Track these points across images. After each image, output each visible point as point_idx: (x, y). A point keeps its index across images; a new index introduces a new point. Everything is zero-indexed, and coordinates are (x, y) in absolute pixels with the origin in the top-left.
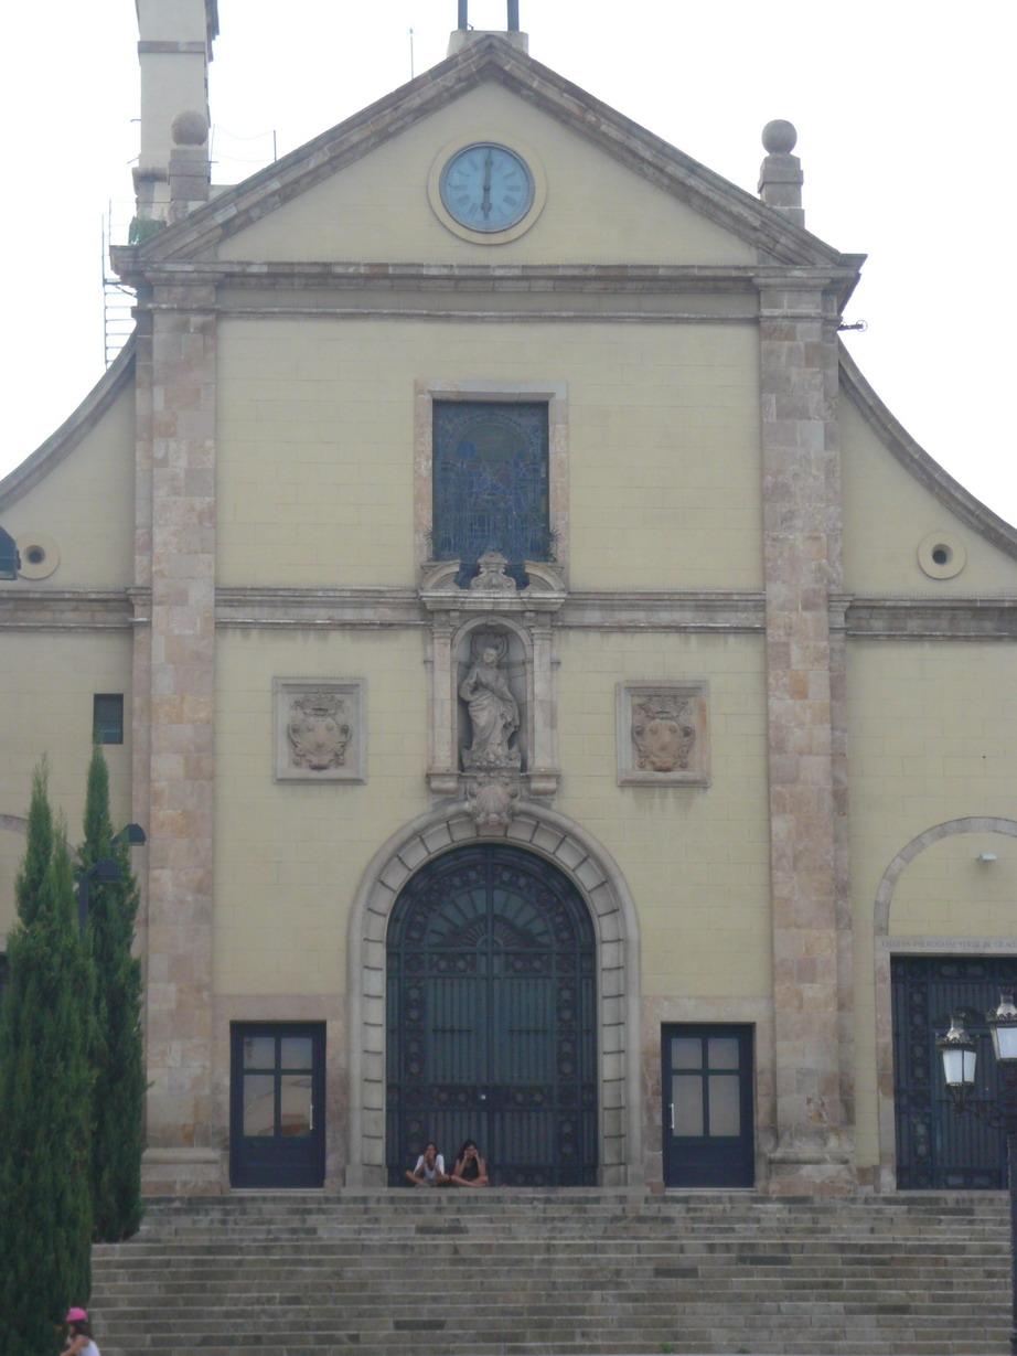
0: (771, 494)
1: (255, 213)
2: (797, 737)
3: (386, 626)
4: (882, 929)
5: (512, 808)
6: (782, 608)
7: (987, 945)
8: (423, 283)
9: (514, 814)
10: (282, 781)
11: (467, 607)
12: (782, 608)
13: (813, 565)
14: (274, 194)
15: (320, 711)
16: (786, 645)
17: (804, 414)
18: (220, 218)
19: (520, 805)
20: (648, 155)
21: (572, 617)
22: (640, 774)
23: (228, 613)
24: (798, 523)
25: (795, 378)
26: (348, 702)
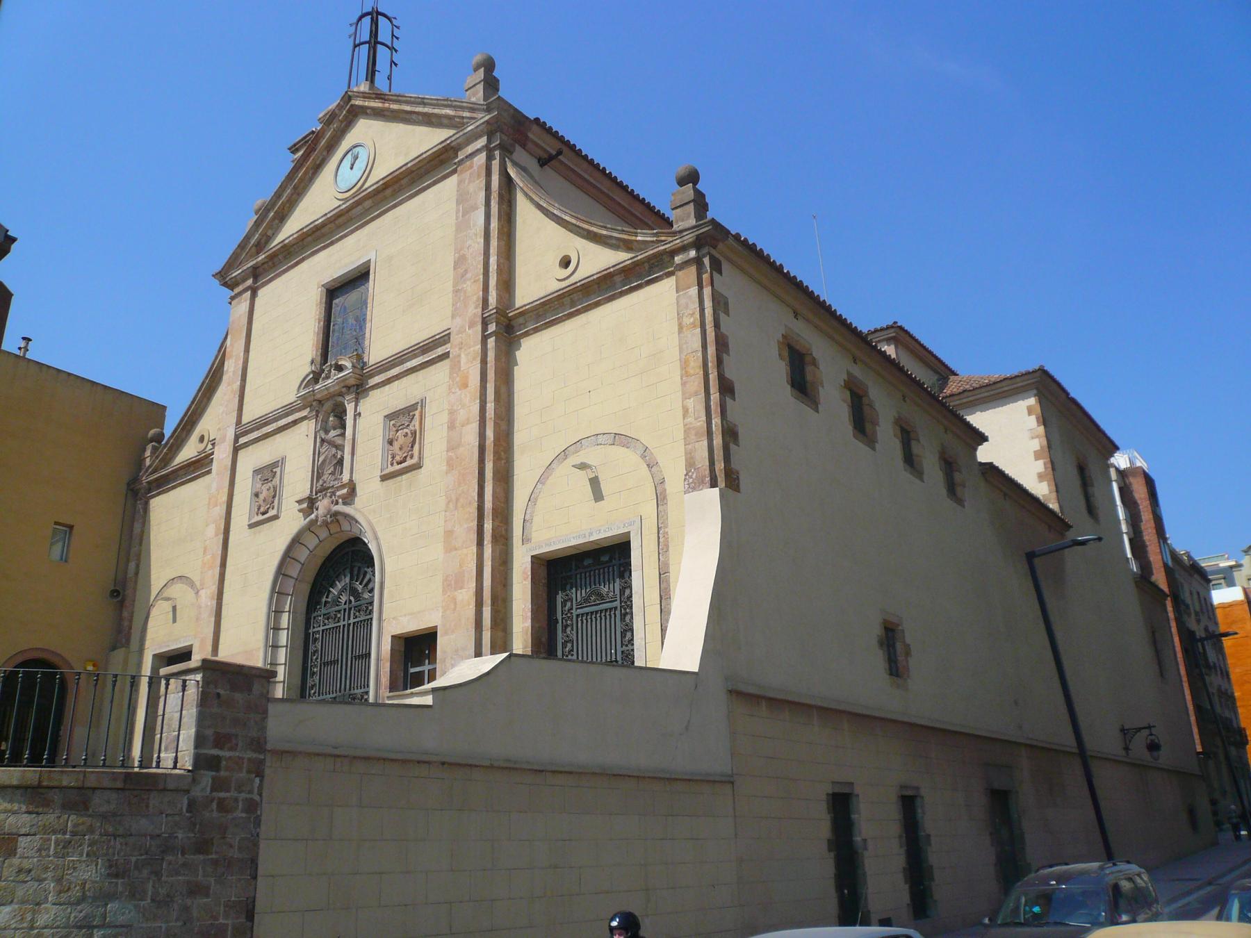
0: (460, 262)
1: (270, 233)
2: (462, 415)
3: (295, 422)
4: (525, 540)
5: (329, 511)
6: (459, 332)
7: (591, 534)
8: (323, 230)
9: (336, 514)
10: (251, 526)
11: (318, 396)
12: (459, 332)
13: (475, 298)
14: (274, 218)
15: (266, 480)
16: (459, 356)
17: (475, 208)
18: (252, 242)
19: (336, 508)
20: (408, 108)
21: (372, 382)
22: (391, 469)
23: (242, 440)
24: (469, 275)
25: (471, 190)
26: (278, 470)
